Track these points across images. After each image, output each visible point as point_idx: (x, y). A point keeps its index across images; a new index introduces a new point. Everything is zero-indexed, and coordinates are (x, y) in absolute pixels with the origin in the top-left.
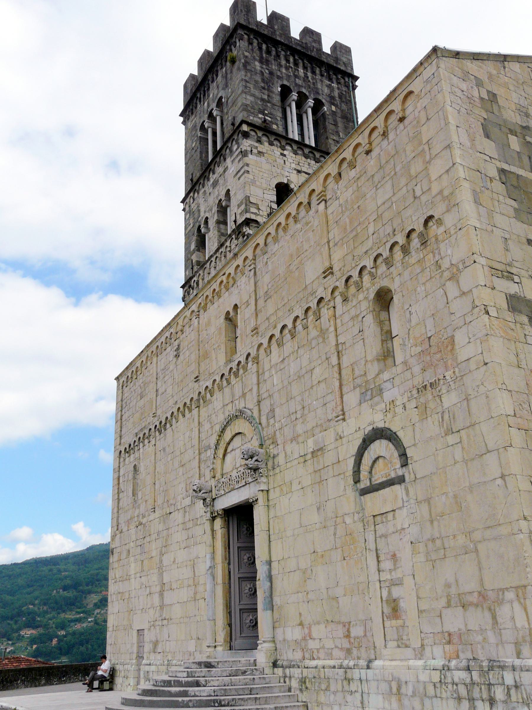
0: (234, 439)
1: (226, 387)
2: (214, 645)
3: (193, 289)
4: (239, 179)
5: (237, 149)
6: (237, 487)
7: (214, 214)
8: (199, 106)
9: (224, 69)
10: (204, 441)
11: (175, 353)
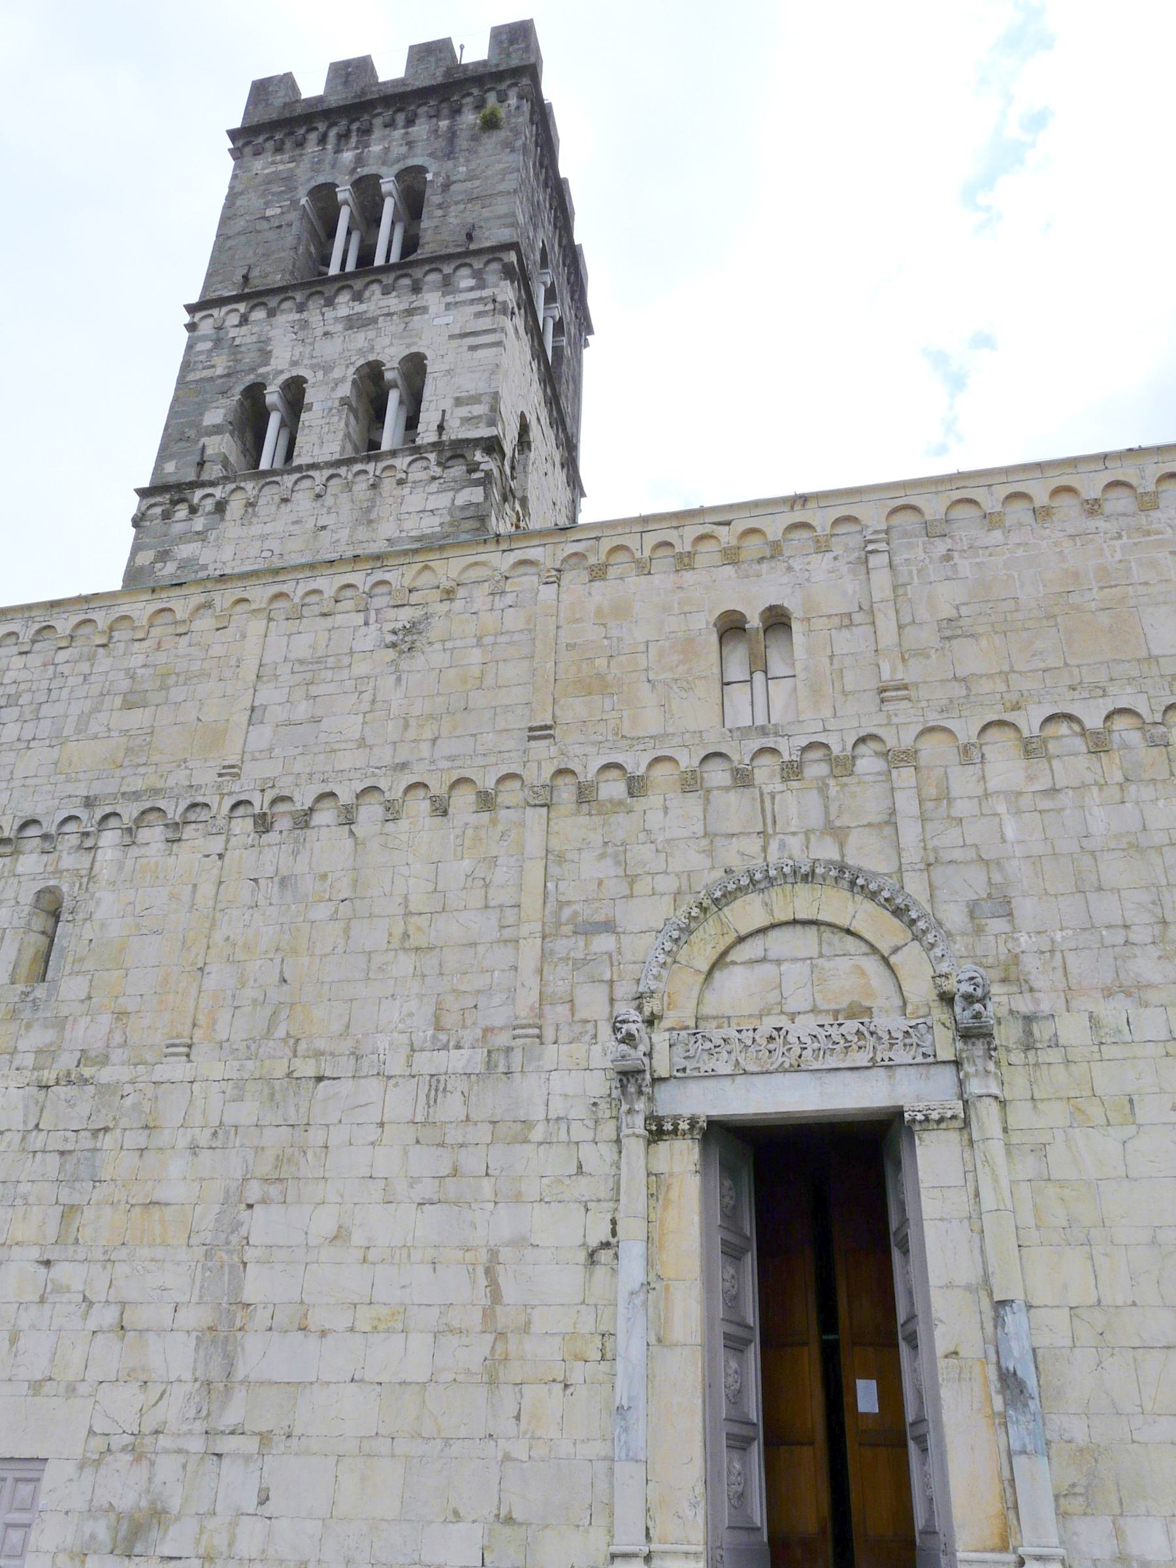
0: (773, 935)
1: (727, 789)
2: (646, 1550)
3: (193, 510)
4: (473, 348)
5: (471, 289)
6: (816, 1066)
7: (337, 383)
8: (312, 148)
9: (444, 124)
10: (576, 907)
11: (390, 638)
